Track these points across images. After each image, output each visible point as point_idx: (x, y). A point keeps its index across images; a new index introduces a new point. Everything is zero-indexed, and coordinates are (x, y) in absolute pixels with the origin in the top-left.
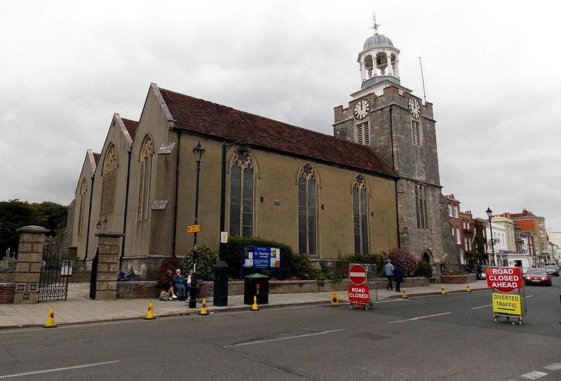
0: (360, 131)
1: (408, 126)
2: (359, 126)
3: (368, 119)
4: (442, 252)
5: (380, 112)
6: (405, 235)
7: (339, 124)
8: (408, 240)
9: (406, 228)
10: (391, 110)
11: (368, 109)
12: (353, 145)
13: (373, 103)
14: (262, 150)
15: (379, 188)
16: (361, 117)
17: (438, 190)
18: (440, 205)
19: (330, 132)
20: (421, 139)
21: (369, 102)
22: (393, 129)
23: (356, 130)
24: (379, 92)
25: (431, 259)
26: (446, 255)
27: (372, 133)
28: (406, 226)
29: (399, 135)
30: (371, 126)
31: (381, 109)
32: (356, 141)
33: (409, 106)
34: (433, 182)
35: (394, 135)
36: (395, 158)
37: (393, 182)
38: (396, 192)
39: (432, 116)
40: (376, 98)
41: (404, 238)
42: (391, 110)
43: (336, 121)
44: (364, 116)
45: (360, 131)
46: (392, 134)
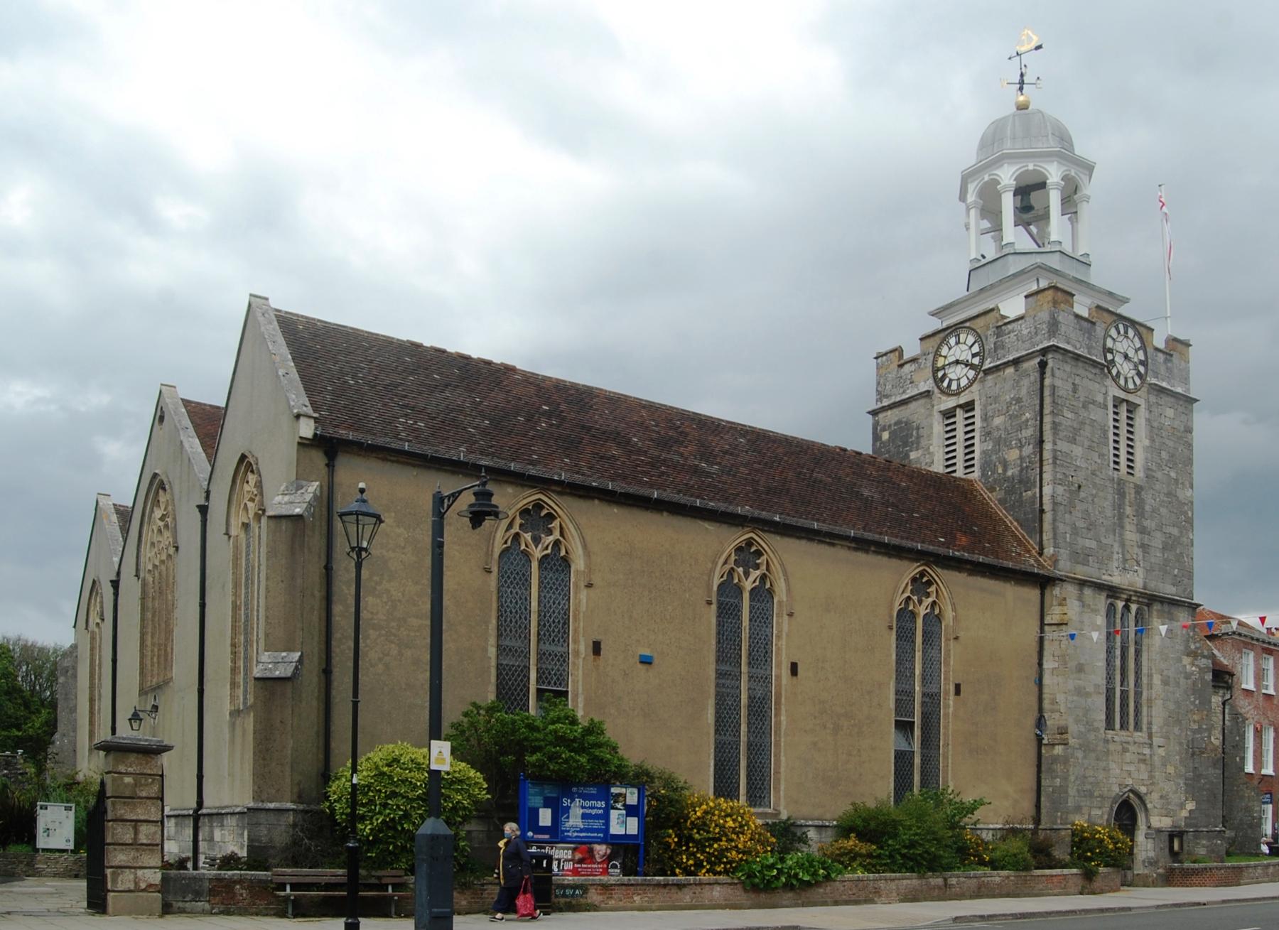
2: (949, 414)
3: (974, 394)
5: (1010, 370)
7: (891, 407)
10: (1043, 365)
11: (976, 361)
16: (954, 387)
21: (979, 339)
22: (1047, 427)
23: (938, 427)
27: (987, 434)
29: (1063, 446)
30: (985, 418)
31: (1016, 362)
35: (1048, 446)
36: (1048, 517)
40: (1002, 326)
42: (1043, 365)
43: (881, 395)
46: (1041, 442)
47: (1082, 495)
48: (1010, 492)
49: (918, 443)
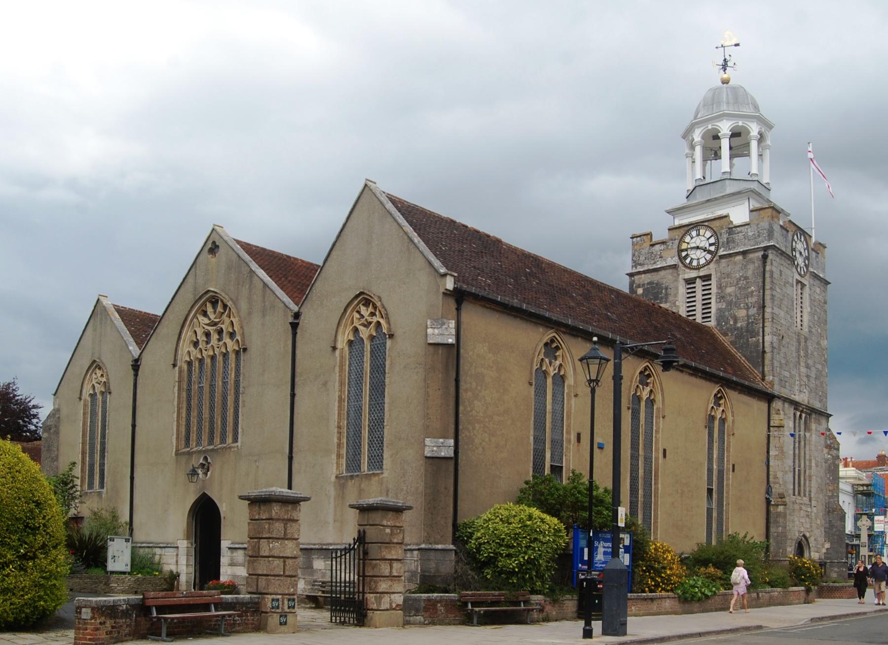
0: (691, 293)
1: (789, 290)
4: (821, 539)
6: (781, 509)
8: (785, 517)
9: (782, 496)
12: (676, 316)
13: (724, 237)
14: (516, 317)
15: (745, 416)
17: (823, 421)
18: (826, 451)
19: (623, 285)
20: (806, 318)
24: (739, 214)
25: (806, 554)
26: (827, 545)
28: (781, 491)
32: (683, 312)
33: (793, 250)
34: (817, 405)
37: (764, 406)
38: (769, 426)
39: (824, 270)
41: (779, 515)
44: (702, 261)
45: (691, 293)
47: (784, 342)
48: (739, 337)
49: (667, 298)
